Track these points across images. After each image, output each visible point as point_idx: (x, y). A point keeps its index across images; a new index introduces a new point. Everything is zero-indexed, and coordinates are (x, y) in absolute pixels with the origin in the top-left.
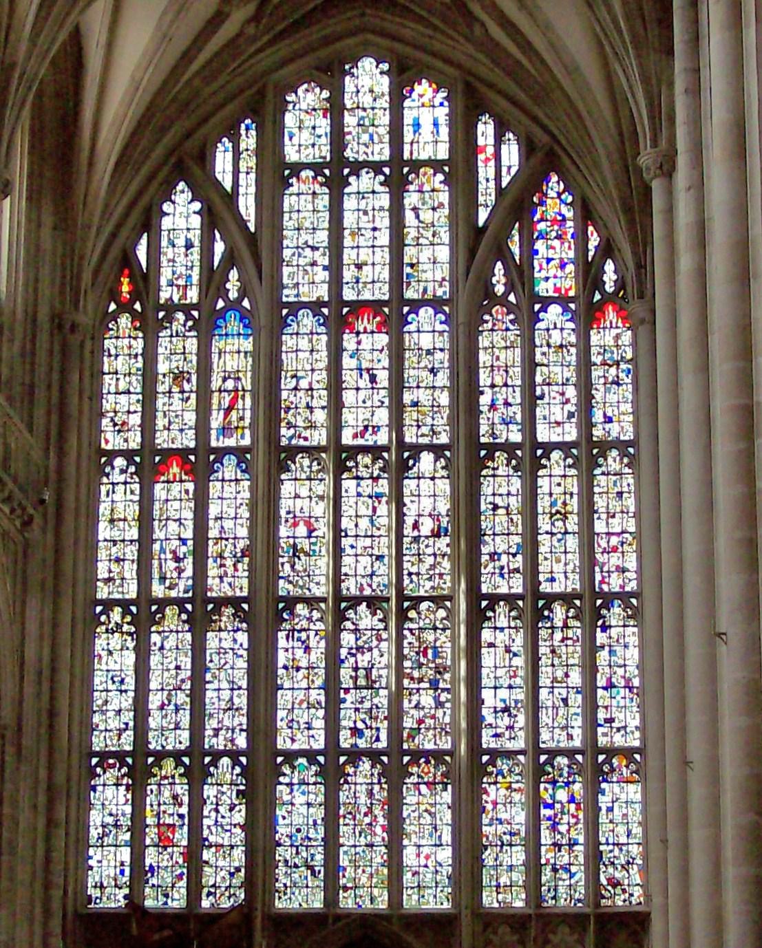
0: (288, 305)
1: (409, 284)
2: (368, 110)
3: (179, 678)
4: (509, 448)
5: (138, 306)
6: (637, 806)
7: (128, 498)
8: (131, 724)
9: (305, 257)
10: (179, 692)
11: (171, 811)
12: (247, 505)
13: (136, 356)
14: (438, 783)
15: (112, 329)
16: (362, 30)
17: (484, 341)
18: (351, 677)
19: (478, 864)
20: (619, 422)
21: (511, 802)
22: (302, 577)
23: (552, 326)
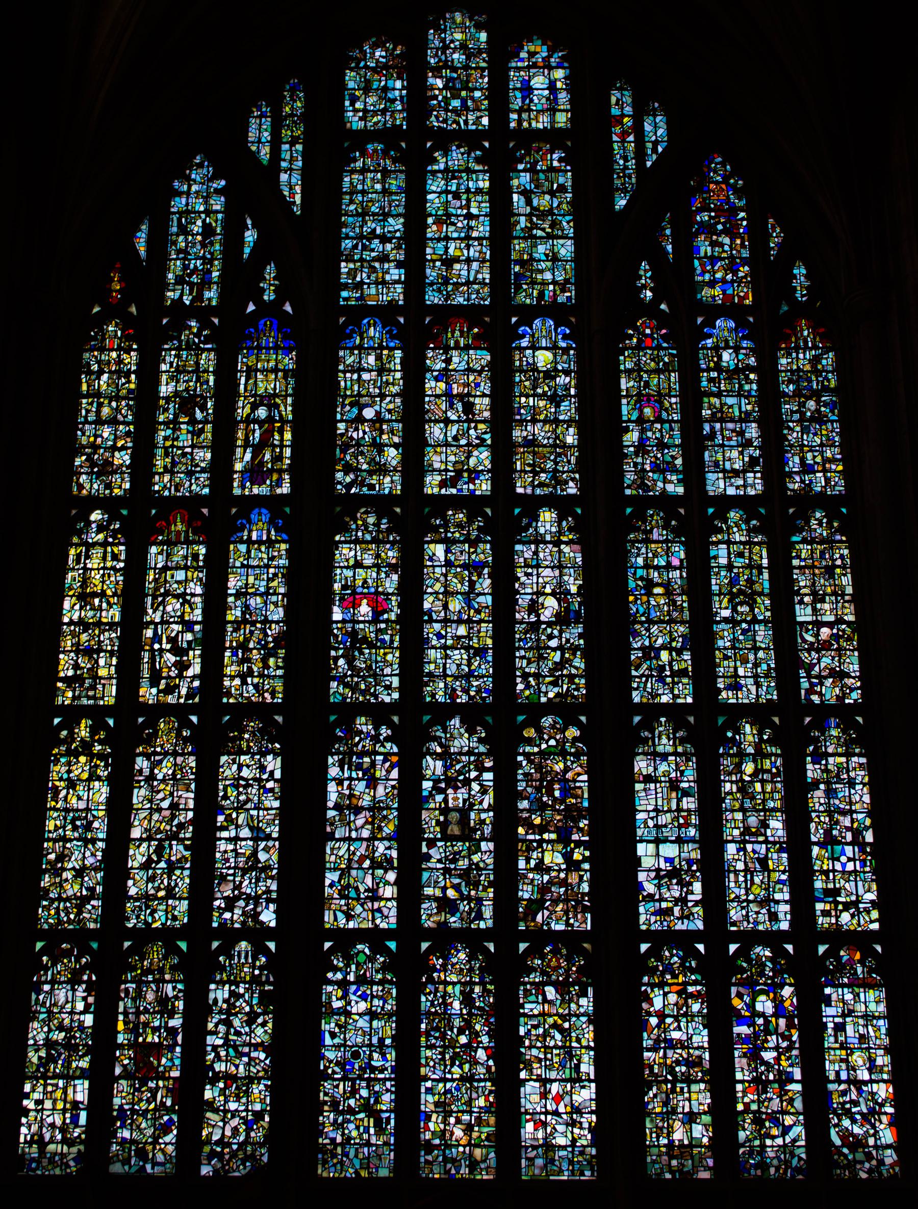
0: (348, 310)
1: (518, 287)
3: (176, 822)
4: (665, 502)
8: (99, 889)
9: (373, 250)
10: (174, 842)
11: (157, 1024)
12: (283, 576)
13: (128, 374)
14: (573, 984)
18: (438, 823)
22: (364, 678)
23: (723, 345)
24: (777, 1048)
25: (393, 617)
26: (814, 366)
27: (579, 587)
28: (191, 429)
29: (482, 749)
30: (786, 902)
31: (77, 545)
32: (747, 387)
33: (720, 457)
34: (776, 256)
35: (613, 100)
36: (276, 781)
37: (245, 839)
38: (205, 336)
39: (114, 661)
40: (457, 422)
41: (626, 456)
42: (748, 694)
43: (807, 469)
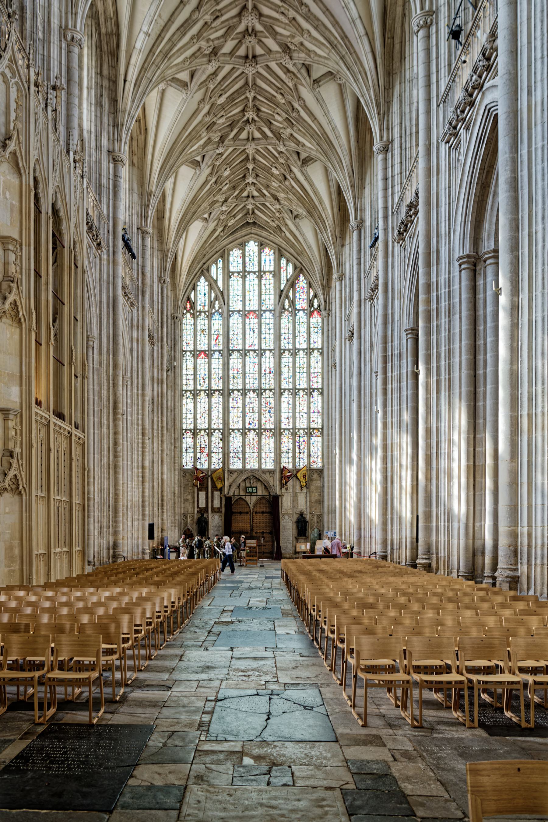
4: (289, 350)
16: (251, 233)
17: (282, 321)
42: (301, 387)
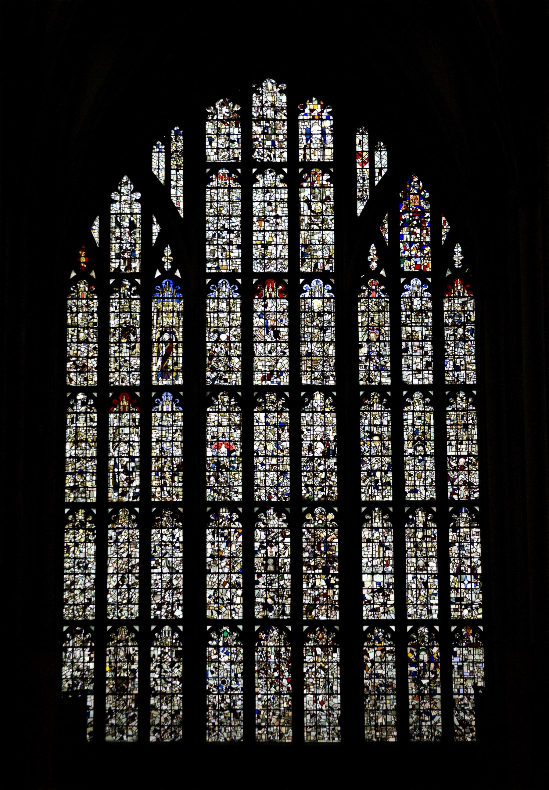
0: (210, 275)
1: (303, 261)
2: (271, 122)
3: (130, 564)
4: (381, 388)
5: (93, 274)
6: (481, 665)
7: (89, 424)
8: (93, 599)
9: (223, 238)
11: (126, 667)
13: (92, 313)
14: (330, 646)
15: (73, 292)
18: (263, 564)
19: (362, 709)
20: (465, 370)
21: (385, 661)
22: (224, 487)
23: (414, 296)
24: (429, 678)
25: (238, 454)
26: (463, 308)
27: (335, 437)
28: (128, 346)
29: (285, 525)
30: (436, 604)
31: (71, 413)
32: (426, 321)
33: (410, 362)
34: (445, 241)
35: (358, 141)
36: (180, 542)
37: (166, 573)
38: (134, 291)
39: (94, 478)
40: (271, 342)
41: (361, 361)
43: (457, 368)
